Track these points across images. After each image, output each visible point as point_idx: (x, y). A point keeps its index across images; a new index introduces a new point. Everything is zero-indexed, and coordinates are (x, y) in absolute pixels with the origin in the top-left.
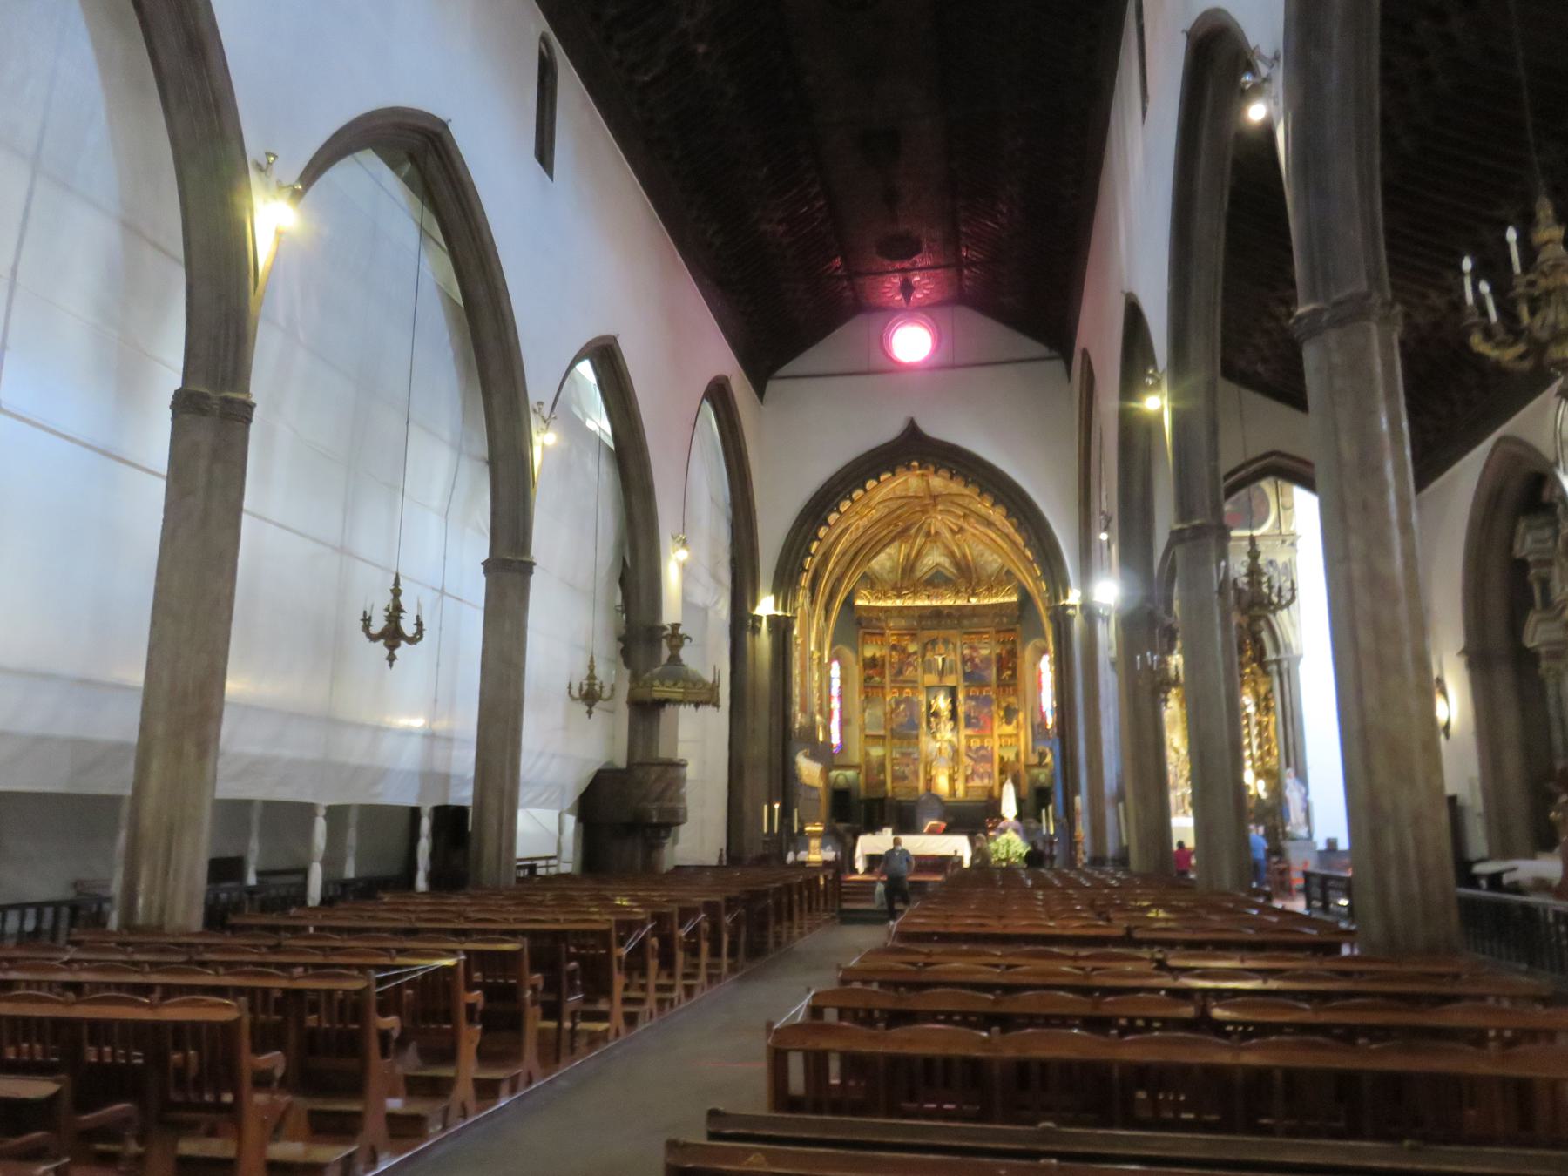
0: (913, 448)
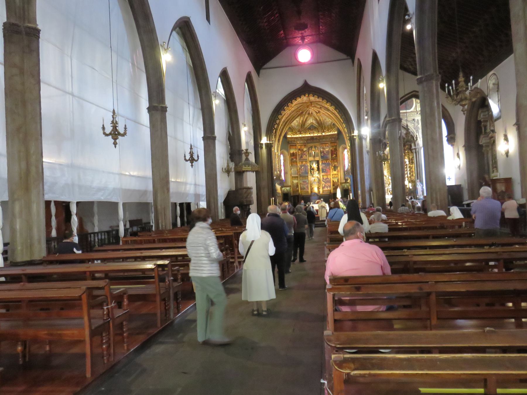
0: (306, 89)
